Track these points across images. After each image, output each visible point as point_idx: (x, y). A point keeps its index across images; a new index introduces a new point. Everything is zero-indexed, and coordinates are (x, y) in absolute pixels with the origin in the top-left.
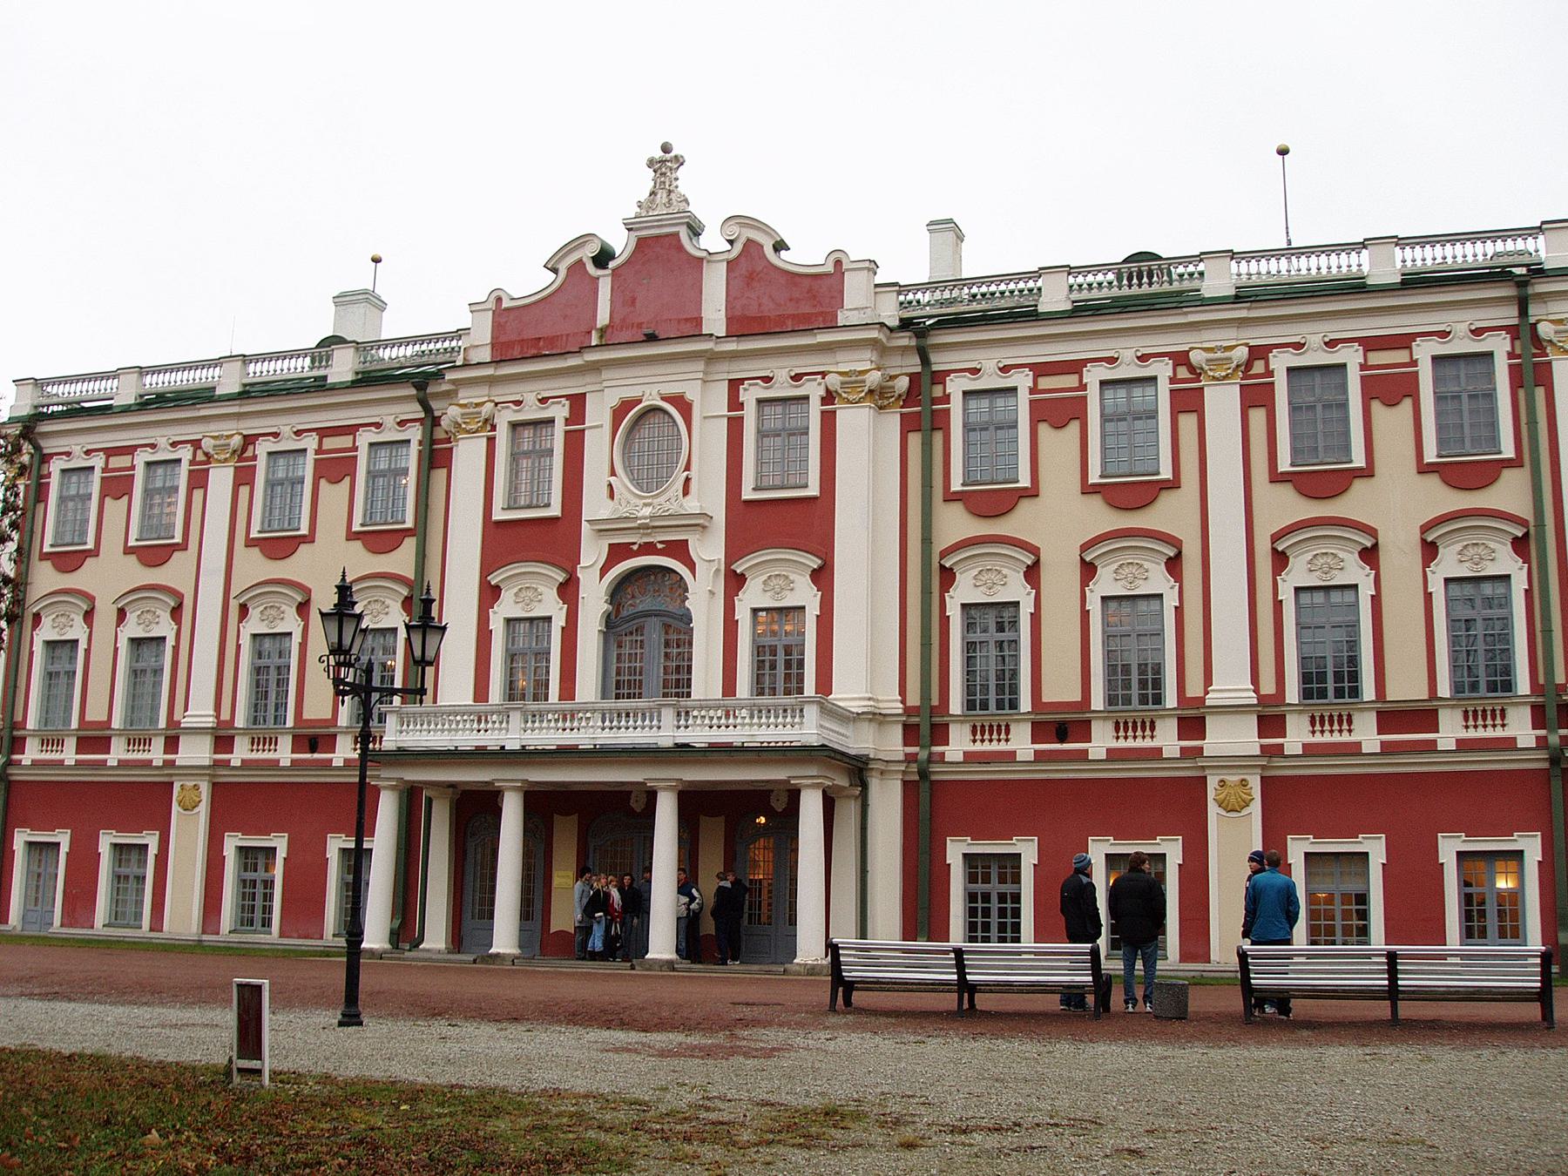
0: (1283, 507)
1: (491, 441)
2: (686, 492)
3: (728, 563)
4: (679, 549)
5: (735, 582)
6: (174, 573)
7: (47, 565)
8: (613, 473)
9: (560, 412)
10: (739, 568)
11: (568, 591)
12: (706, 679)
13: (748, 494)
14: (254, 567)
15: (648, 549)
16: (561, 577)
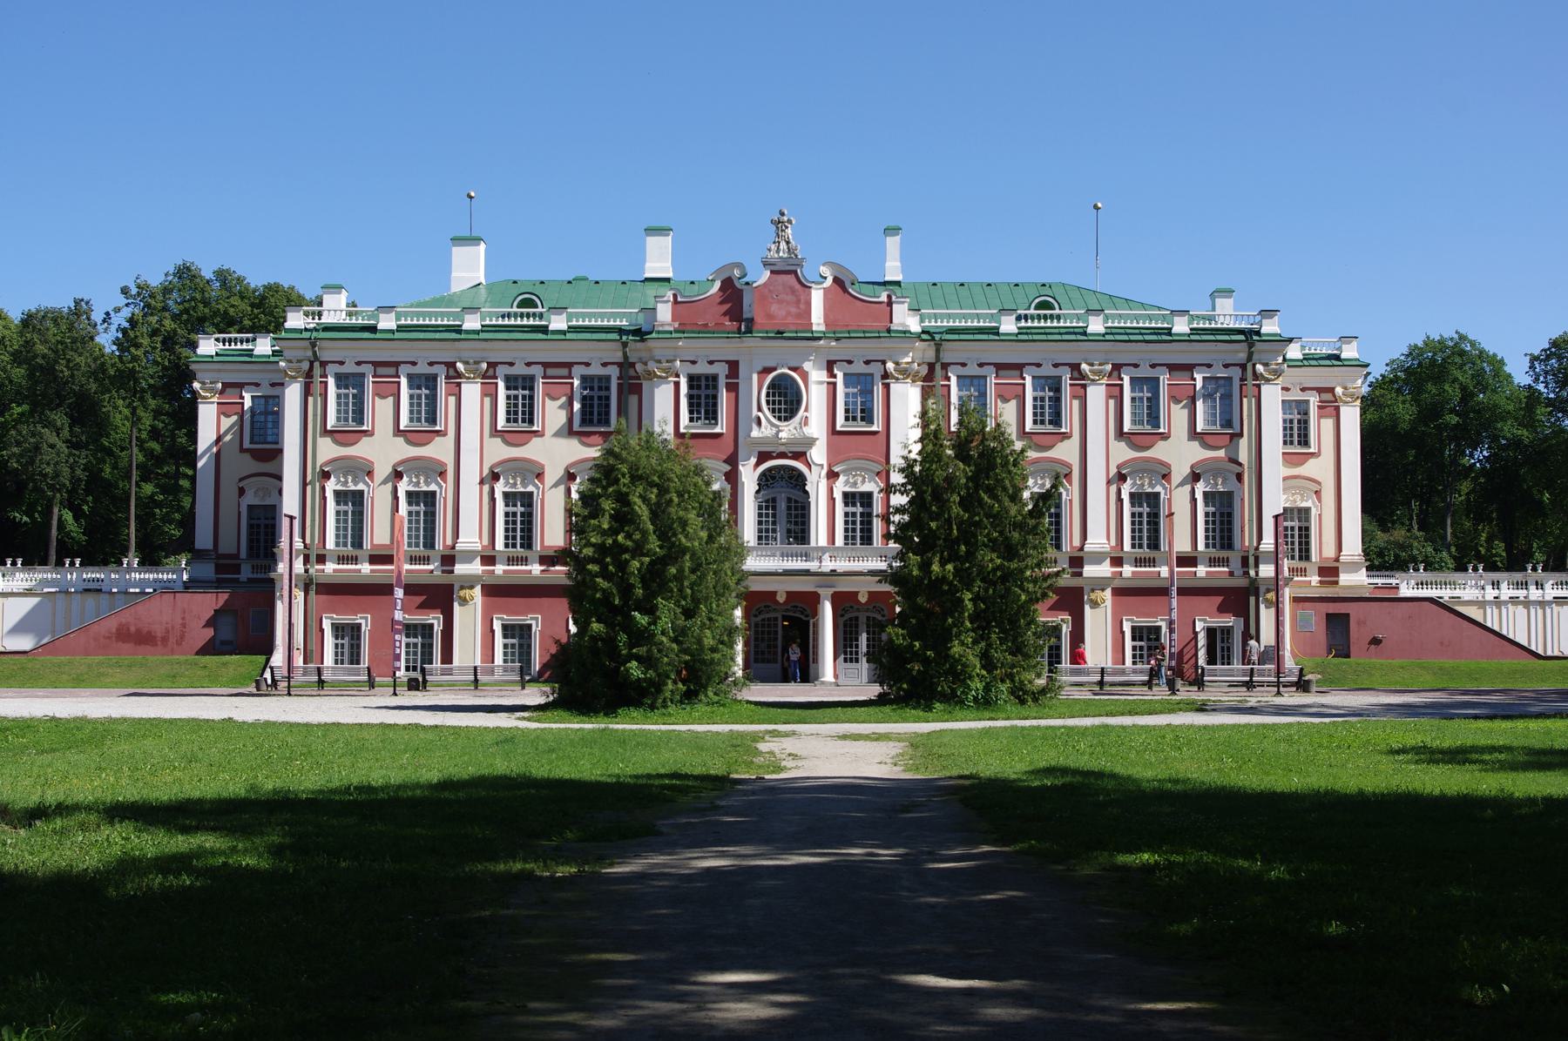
0: (1123, 453)
1: (677, 385)
2: (806, 424)
3: (830, 466)
4: (800, 456)
5: (832, 475)
6: (440, 450)
7: (328, 440)
8: (760, 409)
9: (721, 370)
10: (836, 469)
11: (732, 477)
12: (819, 534)
13: (838, 428)
14: (499, 451)
15: (782, 455)
16: (728, 468)
